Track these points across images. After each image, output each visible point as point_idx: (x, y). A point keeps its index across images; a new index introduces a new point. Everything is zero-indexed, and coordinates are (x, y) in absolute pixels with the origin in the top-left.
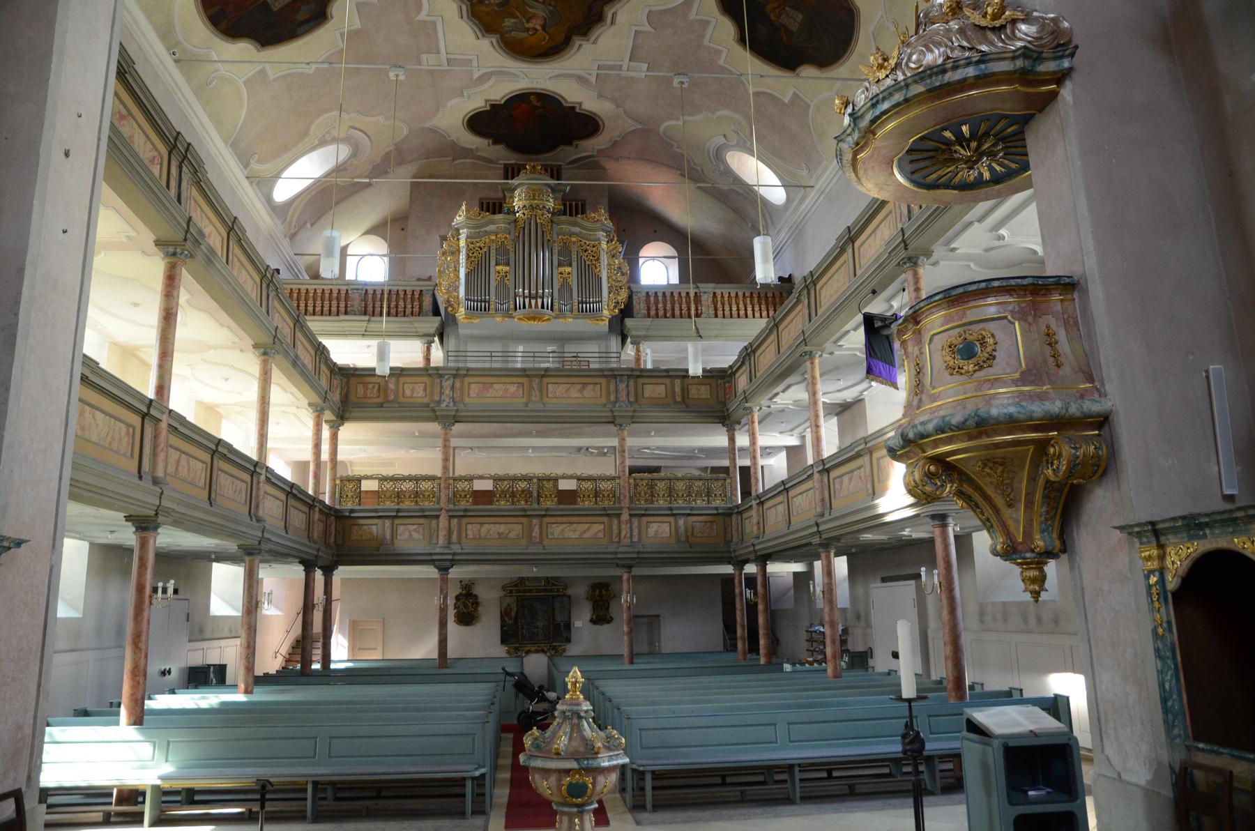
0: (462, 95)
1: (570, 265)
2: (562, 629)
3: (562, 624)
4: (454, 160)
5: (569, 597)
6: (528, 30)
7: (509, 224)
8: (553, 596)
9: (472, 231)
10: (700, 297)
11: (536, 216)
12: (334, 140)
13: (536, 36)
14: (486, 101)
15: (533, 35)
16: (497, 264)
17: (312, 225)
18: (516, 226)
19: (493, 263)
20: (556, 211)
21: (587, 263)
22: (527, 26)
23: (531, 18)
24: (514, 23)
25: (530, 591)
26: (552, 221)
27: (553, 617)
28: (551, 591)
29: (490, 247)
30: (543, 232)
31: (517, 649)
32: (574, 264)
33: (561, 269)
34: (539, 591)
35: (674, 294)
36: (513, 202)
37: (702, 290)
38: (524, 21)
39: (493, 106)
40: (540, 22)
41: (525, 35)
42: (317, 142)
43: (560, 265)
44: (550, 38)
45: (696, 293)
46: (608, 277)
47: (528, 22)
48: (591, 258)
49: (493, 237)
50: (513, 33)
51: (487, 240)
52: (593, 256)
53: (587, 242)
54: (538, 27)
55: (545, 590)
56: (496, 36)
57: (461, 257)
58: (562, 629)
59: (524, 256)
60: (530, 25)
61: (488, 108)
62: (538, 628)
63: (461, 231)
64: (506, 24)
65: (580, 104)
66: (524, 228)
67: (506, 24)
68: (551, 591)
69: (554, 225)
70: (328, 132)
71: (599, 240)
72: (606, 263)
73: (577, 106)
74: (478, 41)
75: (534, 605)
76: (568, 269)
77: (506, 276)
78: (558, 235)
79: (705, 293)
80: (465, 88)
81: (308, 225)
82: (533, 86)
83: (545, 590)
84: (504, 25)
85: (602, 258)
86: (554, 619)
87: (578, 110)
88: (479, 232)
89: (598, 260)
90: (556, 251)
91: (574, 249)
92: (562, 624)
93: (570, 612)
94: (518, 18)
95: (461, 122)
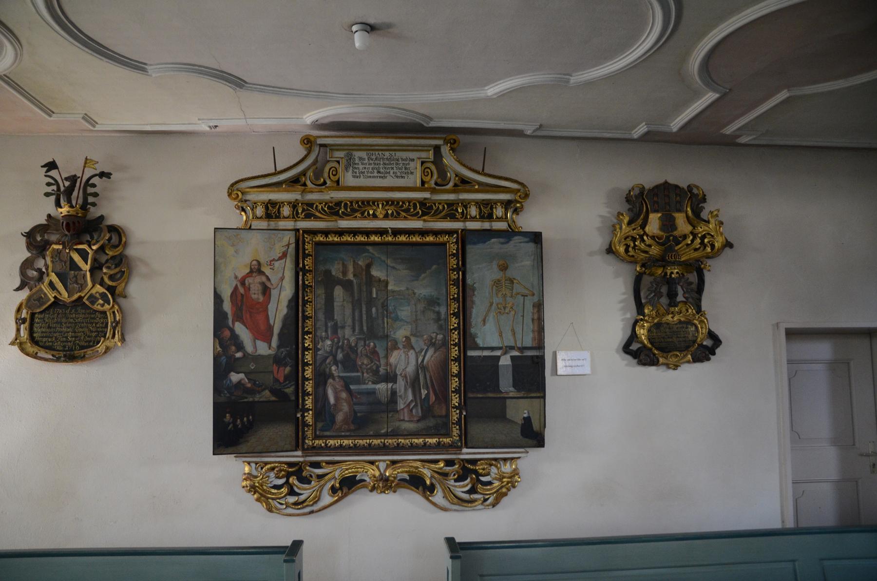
2: (506, 383)
3: (505, 361)
5: (536, 238)
8: (465, 238)
25: (359, 208)
27: (465, 330)
28: (451, 211)
31: (297, 471)
34: (400, 209)
55: (426, 209)
58: (506, 383)
62: (391, 378)
68: (451, 211)
75: (376, 273)
83: (426, 209)
86: (467, 340)
92: (505, 361)
93: (539, 306)
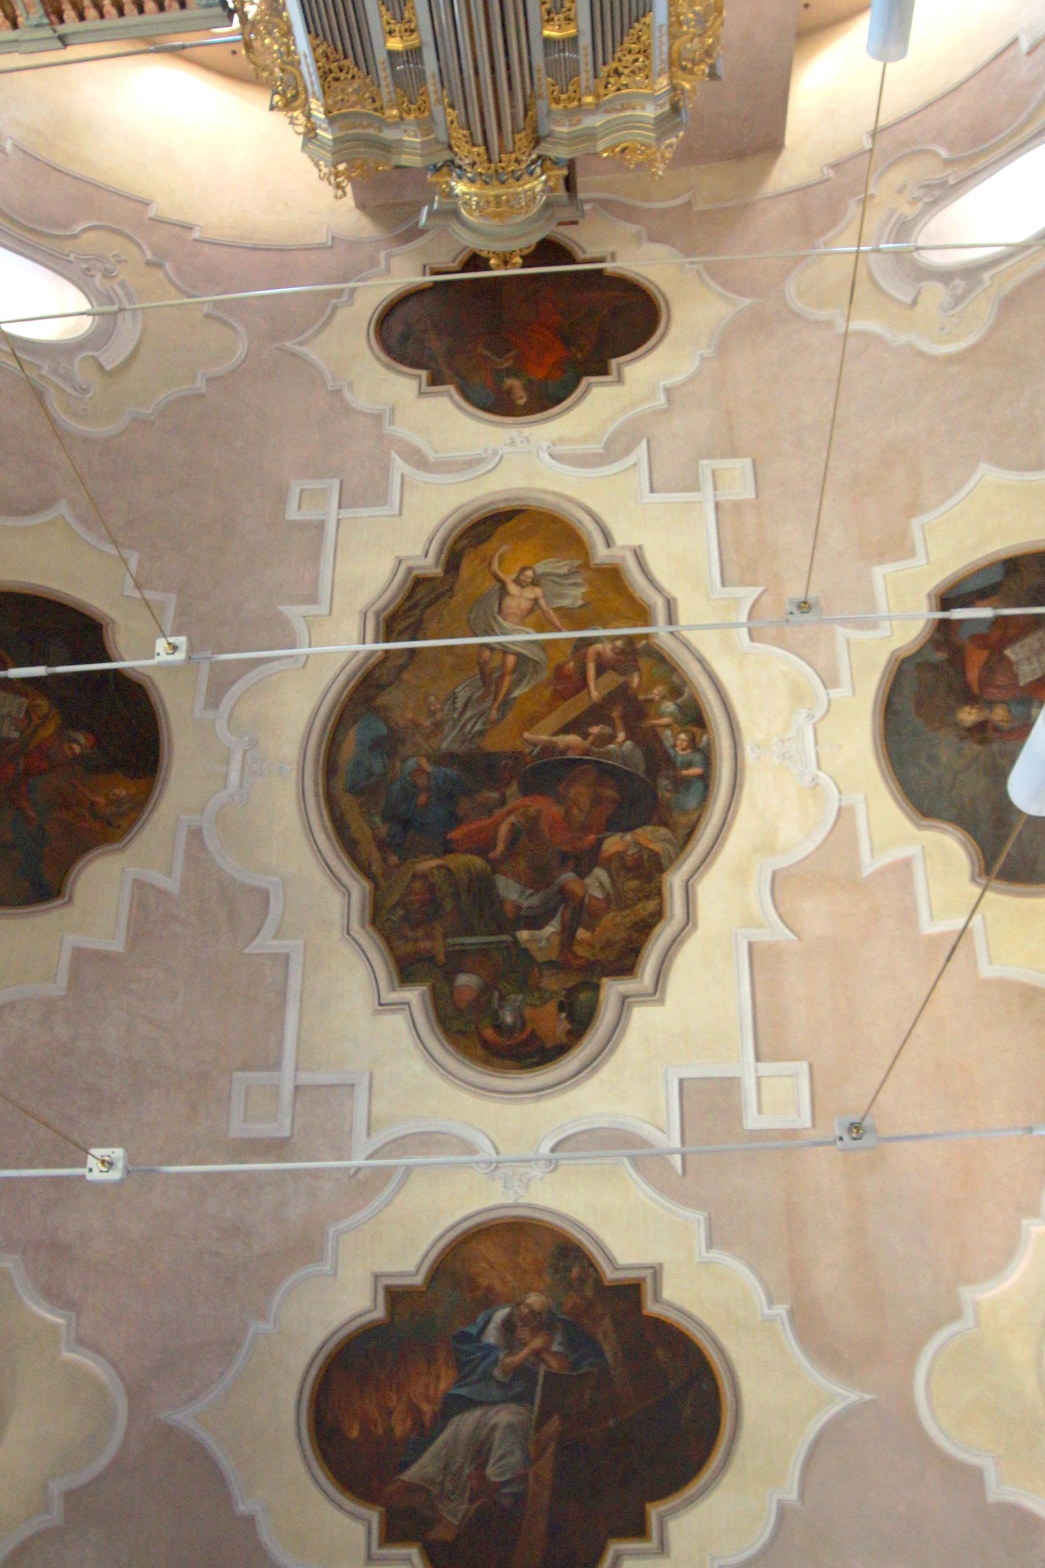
0: (668, 391)
1: (392, 54)
4: (689, 204)
6: (535, 582)
7: (550, 134)
9: (639, 112)
10: (47, 15)
11: (490, 161)
12: (945, 276)
13: (517, 569)
14: (620, 380)
15: (524, 569)
16: (574, 40)
17: (1015, 41)
18: (535, 130)
19: (585, 41)
20: (445, 170)
21: (350, 62)
22: (537, 592)
23: (531, 611)
24: (561, 596)
26: (450, 147)
29: (596, 76)
30: (469, 128)
32: (381, 56)
33: (412, 41)
35: (114, 11)
36: (546, 182)
37: (48, 32)
38: (542, 602)
39: (604, 371)
40: (510, 603)
41: (541, 568)
42: (986, 276)
43: (414, 54)
44: (490, 565)
45: (62, 21)
46: (289, 32)
47: (536, 601)
48: (342, 76)
49: (589, 99)
50: (564, 570)
51: (602, 91)
52: (337, 79)
53: (358, 109)
54: (513, 588)
56: (597, 561)
57: (665, 49)
59: (507, 53)
60: (531, 593)
61: (614, 363)
63: (667, 108)
64: (579, 591)
65: (421, 394)
66: (515, 131)
67: (579, 591)
69: (443, 137)
70: (958, 300)
71: (331, 119)
72: (304, 68)
73: (425, 388)
74: (635, 542)
76: (395, 44)
77: (549, 12)
78: (432, 118)
79: (39, 26)
80: (663, 412)
81: (1024, 45)
82: (527, 431)
84: (583, 590)
85: (315, 78)
87: (424, 374)
88: (623, 108)
89: (324, 75)
90: (430, 81)
91: (387, 90)
94: (556, 610)
95: (677, 315)
